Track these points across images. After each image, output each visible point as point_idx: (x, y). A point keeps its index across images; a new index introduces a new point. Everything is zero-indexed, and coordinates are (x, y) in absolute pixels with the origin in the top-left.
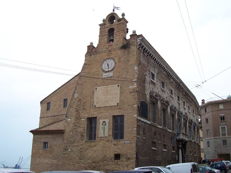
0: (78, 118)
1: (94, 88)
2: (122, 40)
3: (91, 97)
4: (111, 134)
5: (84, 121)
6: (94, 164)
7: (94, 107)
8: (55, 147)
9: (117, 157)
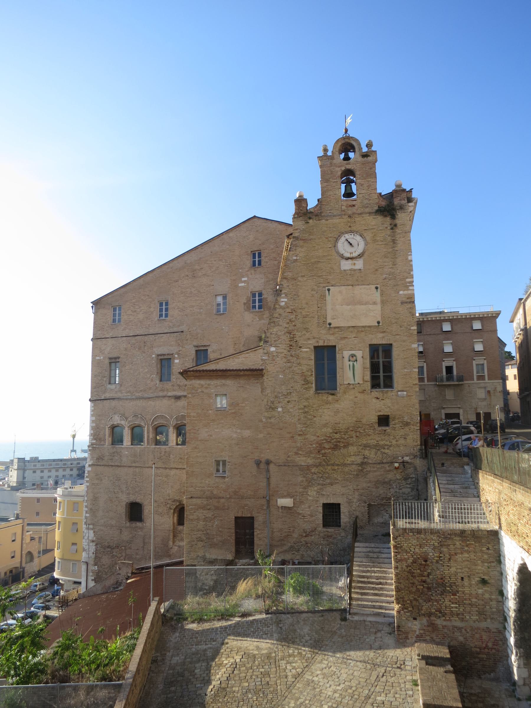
0: (293, 344)
1: (324, 289)
2: (377, 197)
3: (319, 305)
4: (368, 377)
5: (307, 352)
6: (337, 436)
7: (328, 326)
8: (244, 405)
9: (384, 421)
